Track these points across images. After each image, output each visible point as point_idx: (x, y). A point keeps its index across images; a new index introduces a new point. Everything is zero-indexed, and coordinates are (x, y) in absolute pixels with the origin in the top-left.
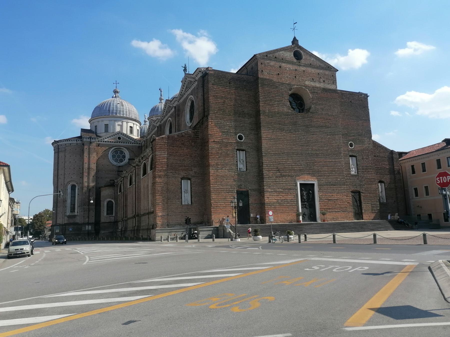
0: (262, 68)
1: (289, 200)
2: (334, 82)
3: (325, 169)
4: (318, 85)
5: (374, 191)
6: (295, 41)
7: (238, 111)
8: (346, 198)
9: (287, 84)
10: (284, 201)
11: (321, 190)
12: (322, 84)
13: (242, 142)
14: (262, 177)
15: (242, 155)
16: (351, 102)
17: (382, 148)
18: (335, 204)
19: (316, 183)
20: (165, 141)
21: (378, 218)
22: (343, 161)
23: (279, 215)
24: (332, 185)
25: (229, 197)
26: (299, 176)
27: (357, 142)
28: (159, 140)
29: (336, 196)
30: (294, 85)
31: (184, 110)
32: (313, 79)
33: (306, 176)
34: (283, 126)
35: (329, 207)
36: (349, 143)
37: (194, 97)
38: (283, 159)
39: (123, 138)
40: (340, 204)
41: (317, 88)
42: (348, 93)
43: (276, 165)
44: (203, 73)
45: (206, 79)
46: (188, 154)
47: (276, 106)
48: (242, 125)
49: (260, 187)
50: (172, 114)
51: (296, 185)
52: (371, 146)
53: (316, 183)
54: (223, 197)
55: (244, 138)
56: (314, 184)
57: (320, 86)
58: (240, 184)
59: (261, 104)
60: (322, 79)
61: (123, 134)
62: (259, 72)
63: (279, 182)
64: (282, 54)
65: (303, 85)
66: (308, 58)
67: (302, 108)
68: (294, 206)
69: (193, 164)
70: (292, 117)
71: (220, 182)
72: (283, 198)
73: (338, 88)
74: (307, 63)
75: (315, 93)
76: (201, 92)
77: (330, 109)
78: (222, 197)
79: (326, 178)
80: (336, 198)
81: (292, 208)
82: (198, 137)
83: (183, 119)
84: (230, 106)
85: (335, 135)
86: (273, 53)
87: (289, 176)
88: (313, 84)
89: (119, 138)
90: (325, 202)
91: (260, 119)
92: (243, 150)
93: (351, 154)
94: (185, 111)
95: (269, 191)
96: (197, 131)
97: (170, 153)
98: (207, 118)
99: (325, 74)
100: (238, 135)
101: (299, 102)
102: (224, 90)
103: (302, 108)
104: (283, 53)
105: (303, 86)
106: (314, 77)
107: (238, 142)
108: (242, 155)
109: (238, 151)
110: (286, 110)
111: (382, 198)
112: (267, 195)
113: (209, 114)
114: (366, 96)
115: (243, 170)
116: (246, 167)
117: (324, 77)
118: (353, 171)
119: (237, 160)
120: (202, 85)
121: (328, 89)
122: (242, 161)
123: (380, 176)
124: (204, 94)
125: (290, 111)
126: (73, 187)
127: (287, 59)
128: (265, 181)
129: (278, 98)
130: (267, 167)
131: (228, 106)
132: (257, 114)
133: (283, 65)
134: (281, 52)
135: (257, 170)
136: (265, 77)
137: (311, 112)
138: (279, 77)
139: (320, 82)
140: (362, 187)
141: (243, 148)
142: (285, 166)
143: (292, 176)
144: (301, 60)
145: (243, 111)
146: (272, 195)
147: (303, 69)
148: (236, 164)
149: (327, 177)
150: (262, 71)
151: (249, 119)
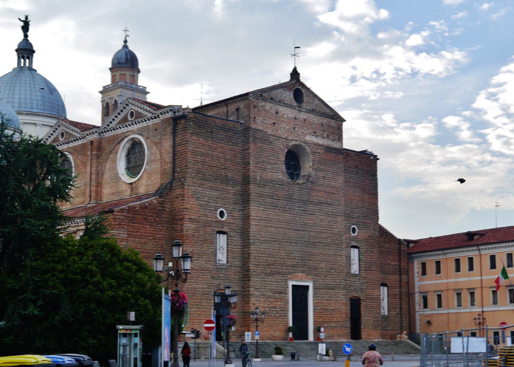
0: (255, 114)
1: (279, 308)
2: (340, 138)
3: (323, 265)
4: (320, 141)
5: (377, 299)
6: (295, 74)
7: (221, 175)
8: (344, 307)
9: (283, 138)
10: (272, 309)
11: (317, 296)
12: (325, 140)
13: (224, 221)
14: (248, 274)
15: (222, 240)
17: (388, 235)
18: (332, 316)
19: (311, 285)
20: (125, 214)
21: (379, 337)
22: (344, 255)
23: (266, 329)
24: (329, 289)
25: (204, 301)
26: (290, 273)
27: (362, 226)
28: (118, 212)
29: (333, 305)
30: (293, 140)
31: (113, 151)
32: (315, 132)
33: (300, 274)
34: (276, 200)
35: (324, 320)
36: (352, 227)
37: (145, 140)
38: (275, 248)
40: (337, 315)
41: (320, 145)
42: (354, 153)
43: (265, 257)
44: (175, 113)
45: (180, 124)
46: (151, 235)
47: (269, 170)
48: (224, 195)
49: (243, 287)
50: (75, 148)
52: (377, 234)
53: (311, 285)
54: (198, 301)
55: (226, 215)
56: (307, 287)
57: (323, 143)
58: (218, 283)
59: (252, 168)
60: (325, 133)
62: (251, 120)
63: (268, 282)
64: (280, 94)
65: (303, 140)
66: (311, 101)
67: (296, 173)
68: (283, 317)
69: (157, 250)
70: (287, 187)
71: (195, 278)
72: (272, 306)
73: (345, 147)
74: (308, 108)
75: (316, 152)
76: (171, 142)
77: (333, 177)
78: (197, 301)
79: (323, 278)
80: (333, 308)
81: (282, 320)
82: (165, 210)
83: (108, 165)
84: (212, 167)
85: (336, 216)
86: (270, 91)
87: (279, 273)
88: (315, 140)
90: (320, 312)
91: (249, 190)
92: (224, 233)
93: (354, 244)
94: (116, 153)
95: (255, 295)
96: (163, 201)
97: (130, 233)
98: (183, 184)
99: (329, 126)
100: (219, 210)
101: (293, 163)
102: (205, 143)
103: (296, 173)
104: (280, 93)
105: (303, 142)
106: (317, 129)
107: (219, 222)
109: (218, 235)
110: (280, 176)
111: (383, 309)
112: (253, 300)
113: (185, 178)
114: (376, 158)
115: (223, 262)
116: (227, 258)
117: (328, 131)
118: (355, 268)
119: (216, 247)
120: (172, 131)
121: (332, 148)
122: (221, 249)
123: (383, 276)
124: (174, 144)
125: (286, 179)
127: (285, 102)
128: (252, 280)
129: (271, 158)
130: (254, 260)
131: (209, 167)
132: (246, 180)
135: (240, 263)
137: (311, 182)
138: (275, 128)
139: (324, 138)
140: (363, 291)
141: (225, 229)
142: (276, 259)
143: (284, 274)
144: (303, 104)
145: (227, 176)
146: (259, 301)
147: (303, 117)
148: (215, 253)
149: (324, 277)
150: (255, 118)
151: (233, 187)
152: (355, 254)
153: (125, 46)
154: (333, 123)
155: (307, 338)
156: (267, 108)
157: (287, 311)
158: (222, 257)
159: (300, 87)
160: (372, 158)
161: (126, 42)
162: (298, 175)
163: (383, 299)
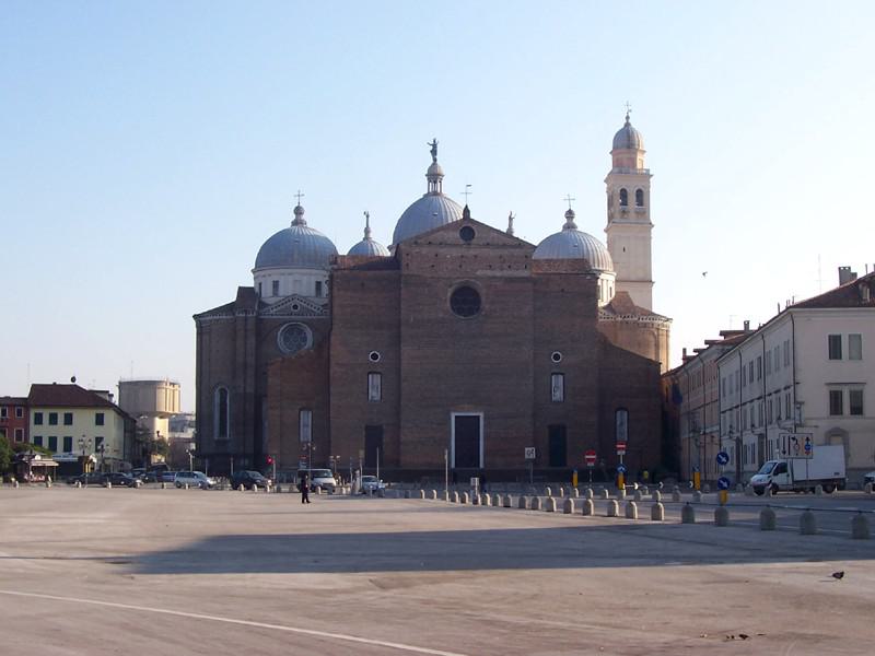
4: (498, 274)
6: (466, 211)
15: (375, 380)
16: (563, 290)
33: (466, 406)
39: (303, 307)
51: (450, 419)
53: (481, 415)
56: (478, 417)
61: (305, 299)
88: (489, 273)
89: (295, 307)
92: (379, 373)
93: (555, 370)
108: (375, 380)
118: (558, 395)
126: (223, 393)
133: (442, 251)
134: (441, 232)
136: (411, 273)
141: (379, 370)
150: (407, 265)
152: (558, 381)
153: (627, 125)
154: (517, 252)
155: (479, 466)
156: (424, 252)
157: (450, 441)
158: (374, 394)
159: (470, 225)
160: (588, 277)
161: (628, 118)
162: (478, 310)
163: (622, 424)
